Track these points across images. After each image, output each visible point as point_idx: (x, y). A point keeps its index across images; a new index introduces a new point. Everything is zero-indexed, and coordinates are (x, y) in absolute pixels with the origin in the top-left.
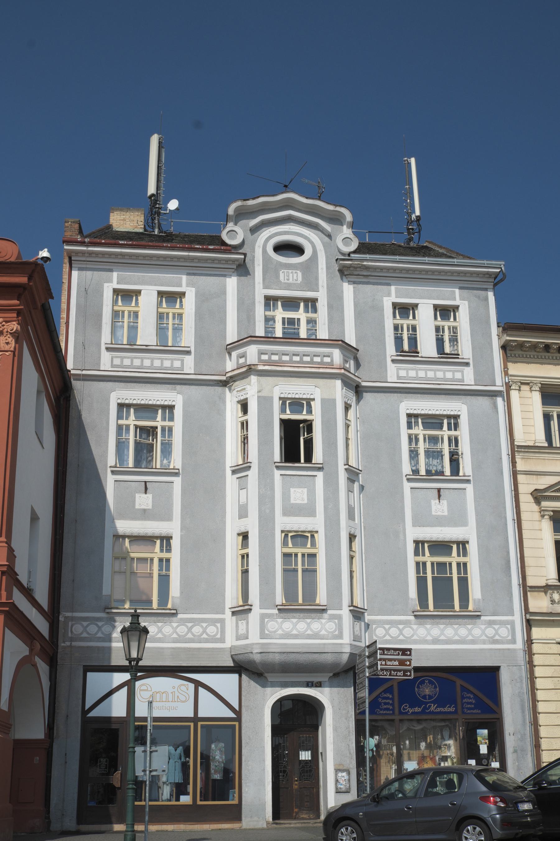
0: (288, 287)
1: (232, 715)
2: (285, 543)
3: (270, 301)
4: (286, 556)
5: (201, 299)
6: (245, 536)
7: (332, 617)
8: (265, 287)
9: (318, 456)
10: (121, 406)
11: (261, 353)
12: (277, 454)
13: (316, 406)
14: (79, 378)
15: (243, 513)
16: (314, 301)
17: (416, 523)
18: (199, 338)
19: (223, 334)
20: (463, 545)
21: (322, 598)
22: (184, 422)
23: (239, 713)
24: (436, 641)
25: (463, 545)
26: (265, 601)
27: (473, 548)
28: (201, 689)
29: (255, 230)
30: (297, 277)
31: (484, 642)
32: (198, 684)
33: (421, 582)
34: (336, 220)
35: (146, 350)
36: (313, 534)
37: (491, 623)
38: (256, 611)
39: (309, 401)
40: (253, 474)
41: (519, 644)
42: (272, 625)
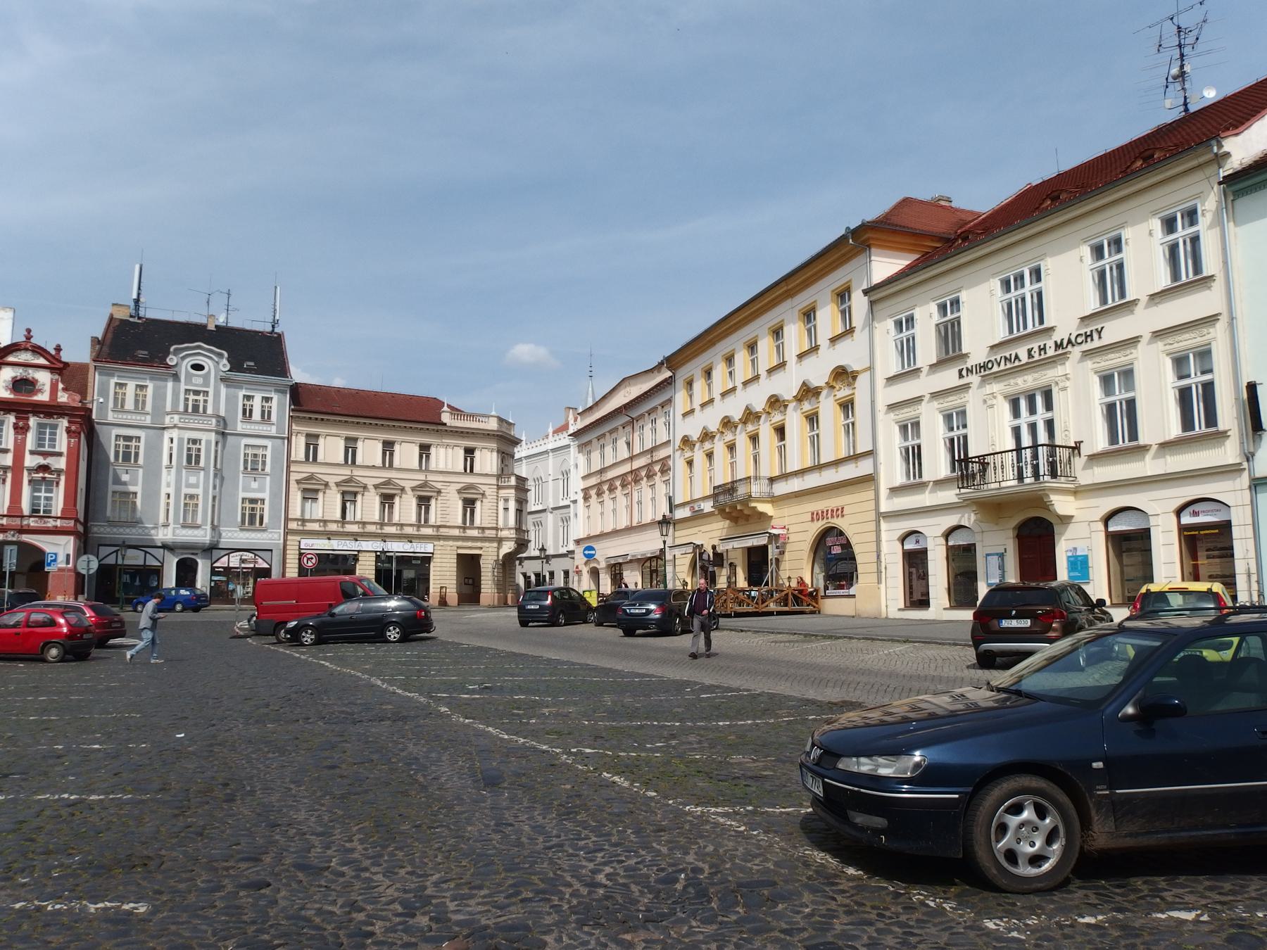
0: (196, 385)
1: (160, 564)
2: (185, 498)
3: (187, 391)
4: (186, 505)
5: (155, 388)
6: (169, 496)
7: (204, 529)
8: (186, 385)
9: (202, 464)
10: (117, 436)
11: (180, 418)
12: (185, 463)
13: (203, 443)
14: (98, 423)
15: (168, 485)
16: (207, 392)
17: (243, 491)
18: (154, 407)
19: (165, 407)
20: (263, 501)
21: (199, 521)
22: (145, 444)
23: (163, 564)
24: (247, 539)
25: (263, 501)
26: (176, 521)
27: (267, 502)
28: (148, 555)
29: (183, 358)
30: (200, 381)
32: (146, 552)
33: (243, 515)
34: (220, 355)
35: (129, 412)
36: (197, 495)
37: (271, 532)
38: (172, 526)
39: (200, 440)
40: (173, 471)
41: (282, 541)
42: (177, 531)
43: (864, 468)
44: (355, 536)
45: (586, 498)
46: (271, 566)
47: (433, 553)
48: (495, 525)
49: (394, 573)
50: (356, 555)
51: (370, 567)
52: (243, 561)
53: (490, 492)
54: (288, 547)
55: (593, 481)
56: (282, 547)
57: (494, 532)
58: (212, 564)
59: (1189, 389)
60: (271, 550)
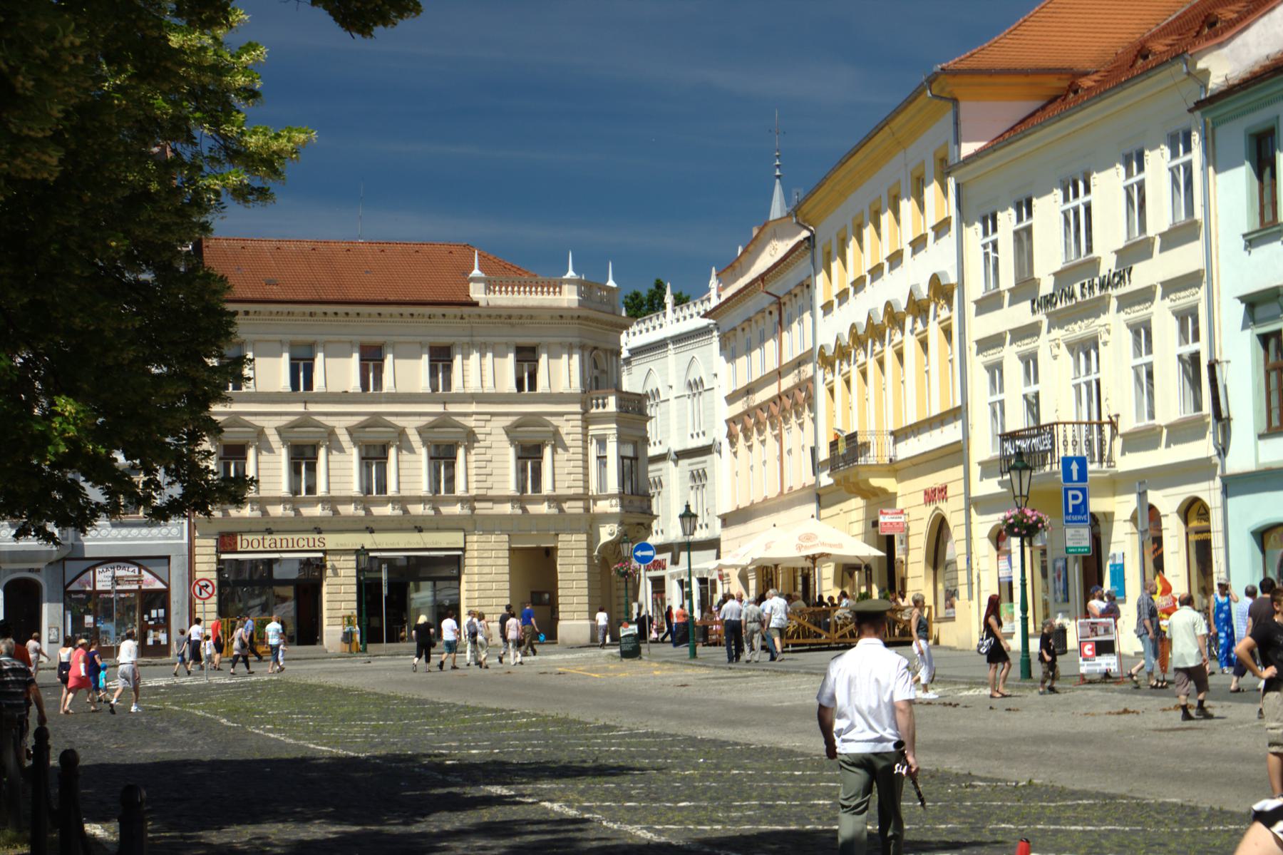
24: (124, 539)
31: (160, 539)
41: (186, 540)
43: (950, 434)
44: (317, 527)
45: (732, 437)
46: (168, 585)
47: (463, 550)
48: (581, 491)
49: (385, 591)
50: (321, 559)
51: (347, 581)
52: (116, 580)
53: (569, 428)
54: (197, 550)
55: (739, 407)
56: (186, 552)
57: (580, 504)
58: (65, 587)
59: (1091, 382)
60: (168, 558)
